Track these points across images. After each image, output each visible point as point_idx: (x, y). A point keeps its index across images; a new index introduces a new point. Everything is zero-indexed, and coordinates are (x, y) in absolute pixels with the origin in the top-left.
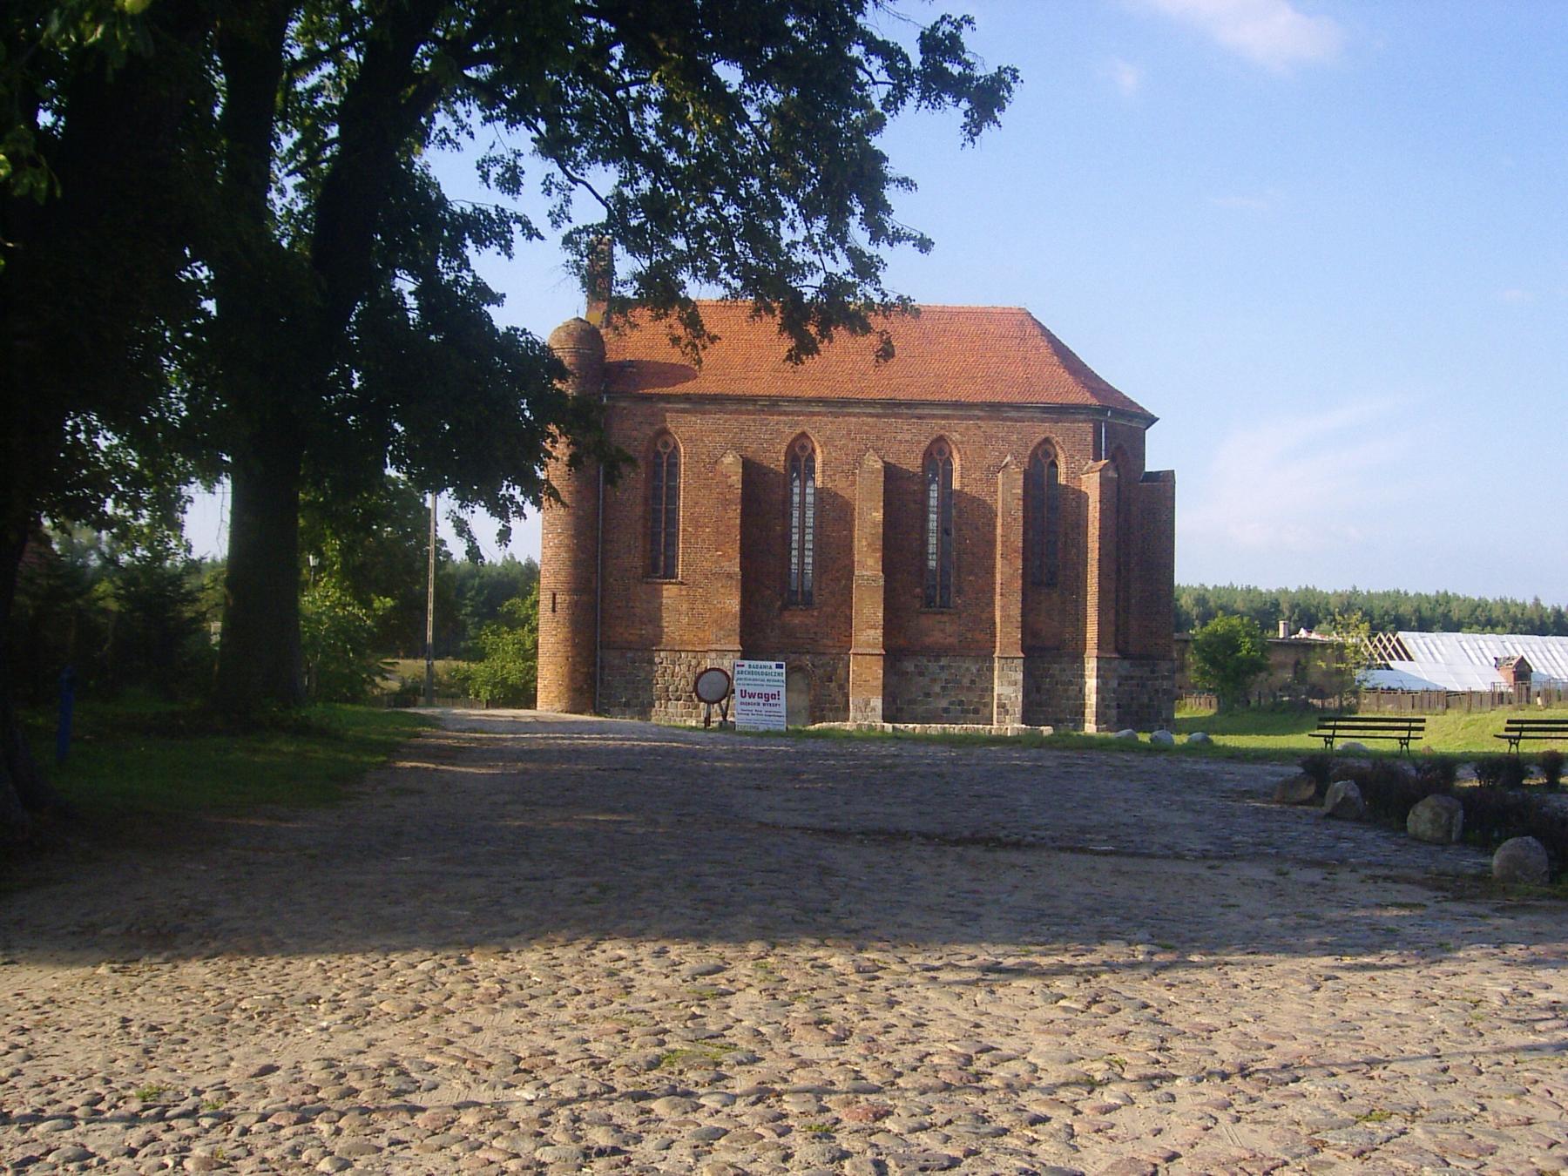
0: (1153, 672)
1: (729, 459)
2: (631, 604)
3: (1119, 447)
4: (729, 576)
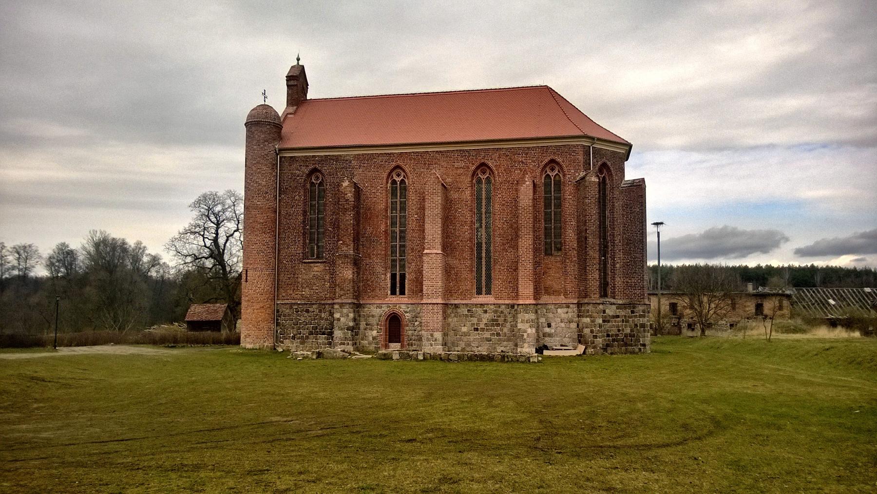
0: (633, 312)
1: (346, 183)
2: (295, 276)
3: (604, 165)
4: (346, 256)
